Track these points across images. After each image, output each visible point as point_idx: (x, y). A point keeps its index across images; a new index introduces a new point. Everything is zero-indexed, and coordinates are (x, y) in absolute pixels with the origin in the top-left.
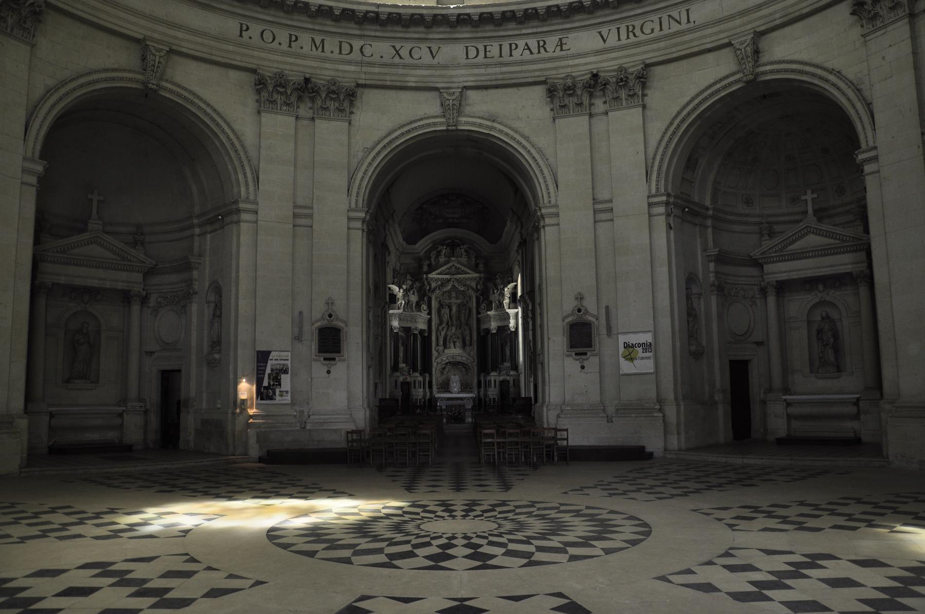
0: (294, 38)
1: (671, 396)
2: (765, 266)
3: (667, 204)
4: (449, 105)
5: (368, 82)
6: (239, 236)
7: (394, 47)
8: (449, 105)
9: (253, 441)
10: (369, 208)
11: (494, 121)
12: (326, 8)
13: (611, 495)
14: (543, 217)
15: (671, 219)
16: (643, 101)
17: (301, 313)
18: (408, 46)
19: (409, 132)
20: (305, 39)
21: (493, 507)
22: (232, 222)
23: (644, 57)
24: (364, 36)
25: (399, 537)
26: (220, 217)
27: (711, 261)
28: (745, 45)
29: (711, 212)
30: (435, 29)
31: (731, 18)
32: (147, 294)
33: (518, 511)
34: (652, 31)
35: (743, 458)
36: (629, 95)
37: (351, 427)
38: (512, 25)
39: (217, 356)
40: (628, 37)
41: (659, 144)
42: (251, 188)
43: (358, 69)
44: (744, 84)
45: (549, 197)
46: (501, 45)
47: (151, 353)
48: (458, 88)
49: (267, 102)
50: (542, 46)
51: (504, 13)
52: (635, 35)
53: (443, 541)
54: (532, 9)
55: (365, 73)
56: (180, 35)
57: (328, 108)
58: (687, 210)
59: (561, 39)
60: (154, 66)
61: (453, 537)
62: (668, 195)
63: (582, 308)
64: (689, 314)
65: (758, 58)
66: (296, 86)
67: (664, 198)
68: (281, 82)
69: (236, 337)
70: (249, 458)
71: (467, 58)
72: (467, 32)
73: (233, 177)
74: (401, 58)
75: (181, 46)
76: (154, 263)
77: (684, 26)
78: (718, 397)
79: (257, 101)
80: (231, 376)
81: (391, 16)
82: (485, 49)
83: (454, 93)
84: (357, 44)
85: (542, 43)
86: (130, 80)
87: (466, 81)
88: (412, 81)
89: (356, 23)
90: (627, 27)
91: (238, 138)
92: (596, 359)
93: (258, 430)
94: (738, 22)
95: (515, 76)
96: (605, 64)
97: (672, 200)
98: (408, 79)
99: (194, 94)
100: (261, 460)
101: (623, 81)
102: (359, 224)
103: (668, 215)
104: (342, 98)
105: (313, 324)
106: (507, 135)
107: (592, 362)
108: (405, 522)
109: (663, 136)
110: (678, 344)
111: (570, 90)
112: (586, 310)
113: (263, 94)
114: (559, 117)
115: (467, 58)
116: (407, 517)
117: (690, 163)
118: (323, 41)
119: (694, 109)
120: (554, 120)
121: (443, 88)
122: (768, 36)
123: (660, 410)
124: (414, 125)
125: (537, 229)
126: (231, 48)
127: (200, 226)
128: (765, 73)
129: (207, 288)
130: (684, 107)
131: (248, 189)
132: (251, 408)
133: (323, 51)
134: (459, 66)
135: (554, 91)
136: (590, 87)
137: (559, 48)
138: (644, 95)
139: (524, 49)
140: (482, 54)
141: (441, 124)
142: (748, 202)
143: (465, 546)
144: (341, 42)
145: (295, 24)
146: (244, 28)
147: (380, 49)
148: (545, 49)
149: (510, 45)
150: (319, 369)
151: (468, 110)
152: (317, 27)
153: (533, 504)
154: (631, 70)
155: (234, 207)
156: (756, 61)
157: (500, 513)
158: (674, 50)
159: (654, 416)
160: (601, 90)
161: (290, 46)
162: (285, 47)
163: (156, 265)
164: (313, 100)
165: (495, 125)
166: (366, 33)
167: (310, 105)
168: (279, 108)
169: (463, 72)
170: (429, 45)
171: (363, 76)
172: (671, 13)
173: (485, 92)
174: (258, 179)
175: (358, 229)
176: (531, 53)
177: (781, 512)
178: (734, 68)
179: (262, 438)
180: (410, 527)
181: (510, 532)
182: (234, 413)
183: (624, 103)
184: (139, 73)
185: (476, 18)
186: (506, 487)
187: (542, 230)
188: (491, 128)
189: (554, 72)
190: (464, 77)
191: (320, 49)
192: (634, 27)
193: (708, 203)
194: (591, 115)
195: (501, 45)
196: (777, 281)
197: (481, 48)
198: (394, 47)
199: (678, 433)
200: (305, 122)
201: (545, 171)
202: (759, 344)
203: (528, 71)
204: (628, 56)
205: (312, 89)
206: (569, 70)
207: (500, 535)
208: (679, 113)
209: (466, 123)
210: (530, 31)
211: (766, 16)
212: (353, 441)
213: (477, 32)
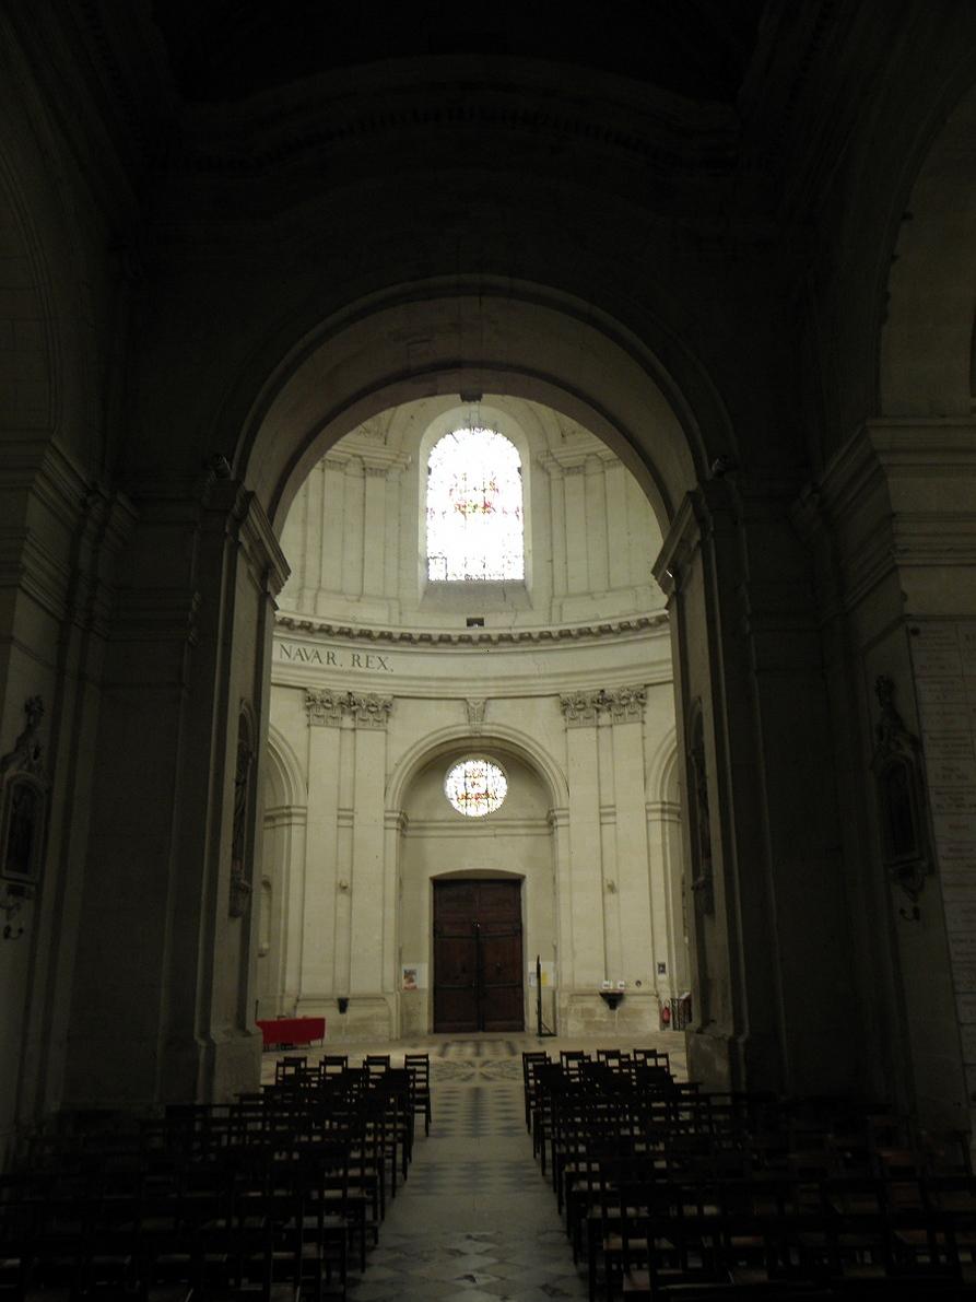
3: (663, 811)
14: (556, 818)
22: (283, 825)
48: (482, 698)
62: (663, 803)
67: (659, 806)
97: (667, 807)
114: (571, 728)
120: (566, 730)
124: (442, 732)
138: (644, 712)
141: (465, 731)
152: (358, 646)
155: (285, 811)
167: (352, 717)
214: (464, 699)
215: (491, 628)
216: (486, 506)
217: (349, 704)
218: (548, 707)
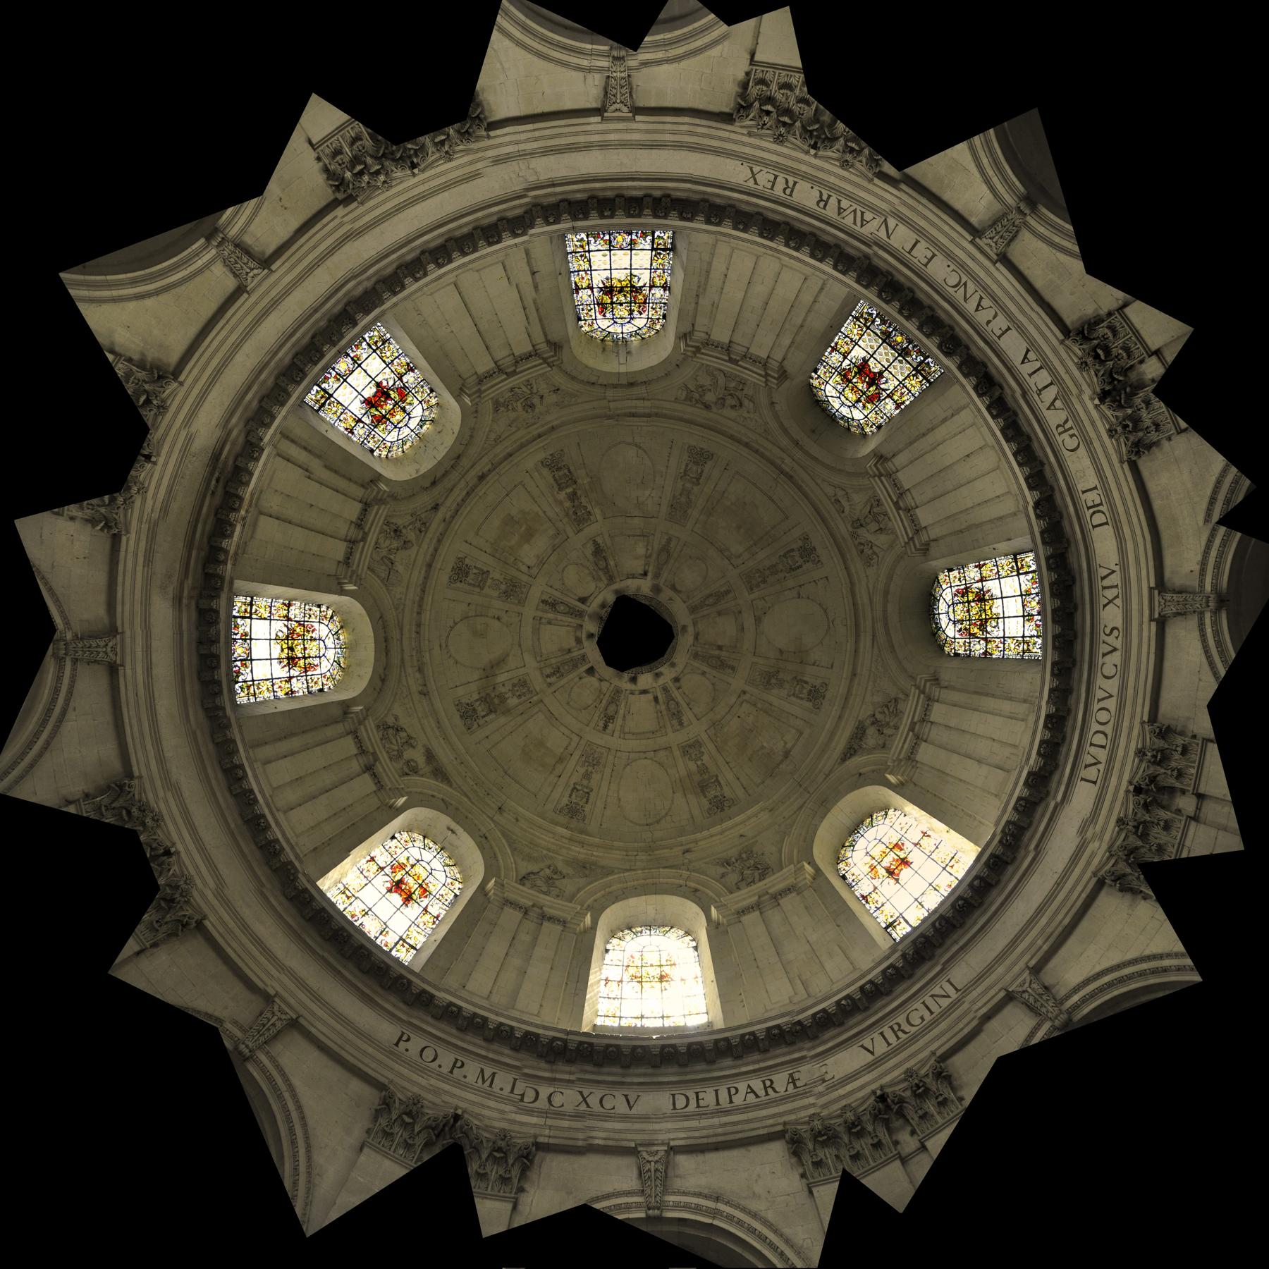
4: (649, 1170)
7: (581, 1093)
8: (649, 1170)
18: (598, 1093)
28: (1027, 985)
46: (716, 1091)
56: (320, 1013)
59: (791, 1075)
60: (264, 1026)
71: (674, 1108)
75: (312, 1025)
82: (697, 1097)
85: (768, 1083)
88: (599, 1138)
94: (1001, 970)
95: (739, 1128)
98: (594, 1134)
115: (674, 1108)
126: (370, 1050)
128: (1076, 1007)
134: (663, 1118)
137: (791, 1086)
141: (638, 1206)
149: (729, 1089)
151: (678, 1184)
169: (669, 1125)
176: (757, 1096)
188: (716, 1213)
190: (673, 1132)
195: (716, 1091)
197: (692, 1095)
198: (581, 1093)
210: (750, 1068)
211: (1028, 948)
213: (686, 1074)
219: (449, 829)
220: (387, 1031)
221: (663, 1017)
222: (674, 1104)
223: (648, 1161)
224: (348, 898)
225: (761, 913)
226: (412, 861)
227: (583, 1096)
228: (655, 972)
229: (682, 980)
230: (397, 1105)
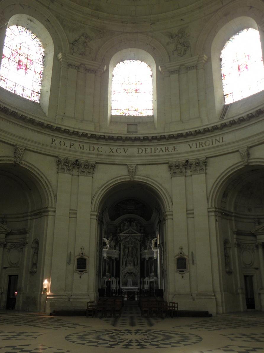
0: (72, 144)
1: (219, 290)
2: (257, 236)
3: (215, 211)
4: (131, 171)
5: (100, 162)
6: (48, 220)
9: (48, 306)
10: (99, 210)
11: (148, 178)
12: (85, 134)
13: (191, 329)
14: (167, 216)
15: (217, 218)
16: (205, 171)
17: (71, 252)
18: (116, 148)
19: (115, 181)
20: (76, 144)
21: (146, 332)
22: (45, 216)
23: (205, 155)
24: (99, 144)
25: (112, 340)
26: (40, 213)
27: (234, 234)
28: (244, 151)
29: (234, 214)
30: (126, 142)
31: (238, 141)
32: (6, 243)
33: (155, 333)
34: (209, 144)
35: (248, 317)
36: (200, 169)
37: (89, 300)
38: (156, 141)
39: (35, 270)
40: (200, 147)
41: (212, 188)
42: (54, 202)
43: (96, 156)
44: (244, 166)
45: (169, 208)
46: (151, 149)
47: (5, 268)
48: (135, 165)
49: (61, 169)
50: (167, 149)
51: (152, 137)
52: (202, 146)
53: (128, 341)
54: (163, 135)
55: (99, 158)
57: (84, 171)
58: (223, 214)
59: (174, 147)
61: (132, 340)
62: (216, 208)
63: (182, 252)
64: (225, 256)
65: (249, 156)
66: (72, 163)
67: (214, 209)
68: (67, 162)
69: (44, 262)
70: (46, 313)
71: (138, 153)
72: (139, 143)
73: (46, 198)
74: (113, 152)
76: (11, 230)
77: (221, 143)
78: (239, 291)
79: (57, 168)
80: (41, 278)
81: (110, 137)
83: (133, 167)
84: (96, 147)
85: (167, 148)
86: (10, 160)
87: (138, 162)
88: (117, 162)
89: (96, 139)
90: (200, 143)
91: (49, 183)
92: (188, 274)
93: (51, 302)
94: (241, 143)
96: (191, 157)
97: (217, 210)
98: (115, 161)
99: (33, 166)
100: (51, 314)
101: (198, 164)
102: (95, 217)
103: (216, 216)
104: (90, 168)
105: (75, 257)
106: (153, 183)
107: (186, 275)
108: (114, 335)
109: (213, 185)
110: (221, 268)
111: (177, 166)
112: (184, 253)
113: (59, 166)
115: (138, 153)
116: (114, 334)
117: (225, 195)
118: (83, 145)
119: (225, 175)
120: (171, 178)
121: (129, 165)
122: (252, 148)
123: (214, 296)
125: (164, 220)
126: (48, 148)
127: (31, 216)
129: (32, 242)
130: (221, 174)
131: (52, 202)
132: (48, 292)
133: (83, 149)
135: (171, 166)
136: (185, 165)
137: (173, 150)
138: (206, 169)
139: (160, 150)
140: (144, 152)
141: (128, 178)
142: (250, 210)
143: (136, 342)
144: (90, 146)
145: (73, 139)
146: (53, 140)
147: (105, 149)
148: (168, 150)
150: (77, 276)
152: (81, 140)
153: (161, 331)
154: (201, 159)
155: (46, 209)
156: (249, 158)
157: (148, 333)
158: (217, 152)
159: (211, 298)
160: (189, 167)
161: (71, 147)
162: (68, 148)
163: (11, 231)
164: (78, 168)
165: (149, 179)
166: (100, 143)
167: (77, 170)
168: (65, 171)
169: (137, 158)
170: (124, 148)
171: (98, 159)
172: (216, 138)
173: (145, 166)
174: (56, 198)
175: (95, 219)
176: (163, 152)
177: (253, 336)
178: (240, 160)
179: (52, 305)
180: (116, 337)
181: (152, 339)
182: (41, 294)
183: (198, 172)
184: (13, 157)
185: (142, 138)
186: (151, 325)
187: (166, 220)
188: (147, 180)
189: (171, 159)
190: (137, 160)
191: (82, 148)
192: (202, 143)
193: (232, 210)
194: (185, 176)
195: (151, 149)
196: (262, 243)
197: (144, 150)
198: (110, 148)
199: (222, 306)
200: (76, 177)
201: (168, 197)
202: (257, 269)
203: (162, 159)
204: (200, 154)
205: (79, 164)
206: (177, 159)
207: (148, 340)
208: (219, 177)
209: (137, 178)
210: (162, 143)
212: (90, 306)
214: (126, 165)
215: (140, 134)
216: (136, 90)
217: (77, 164)
218: (166, 167)
219: (29, 19)
220: (48, 139)
221: (136, 110)
222: (138, 152)
223: (131, 169)
224: (4, 80)
225: (179, 75)
226: (19, 46)
227: (112, 151)
228: (134, 87)
229: (144, 92)
230: (62, 161)
